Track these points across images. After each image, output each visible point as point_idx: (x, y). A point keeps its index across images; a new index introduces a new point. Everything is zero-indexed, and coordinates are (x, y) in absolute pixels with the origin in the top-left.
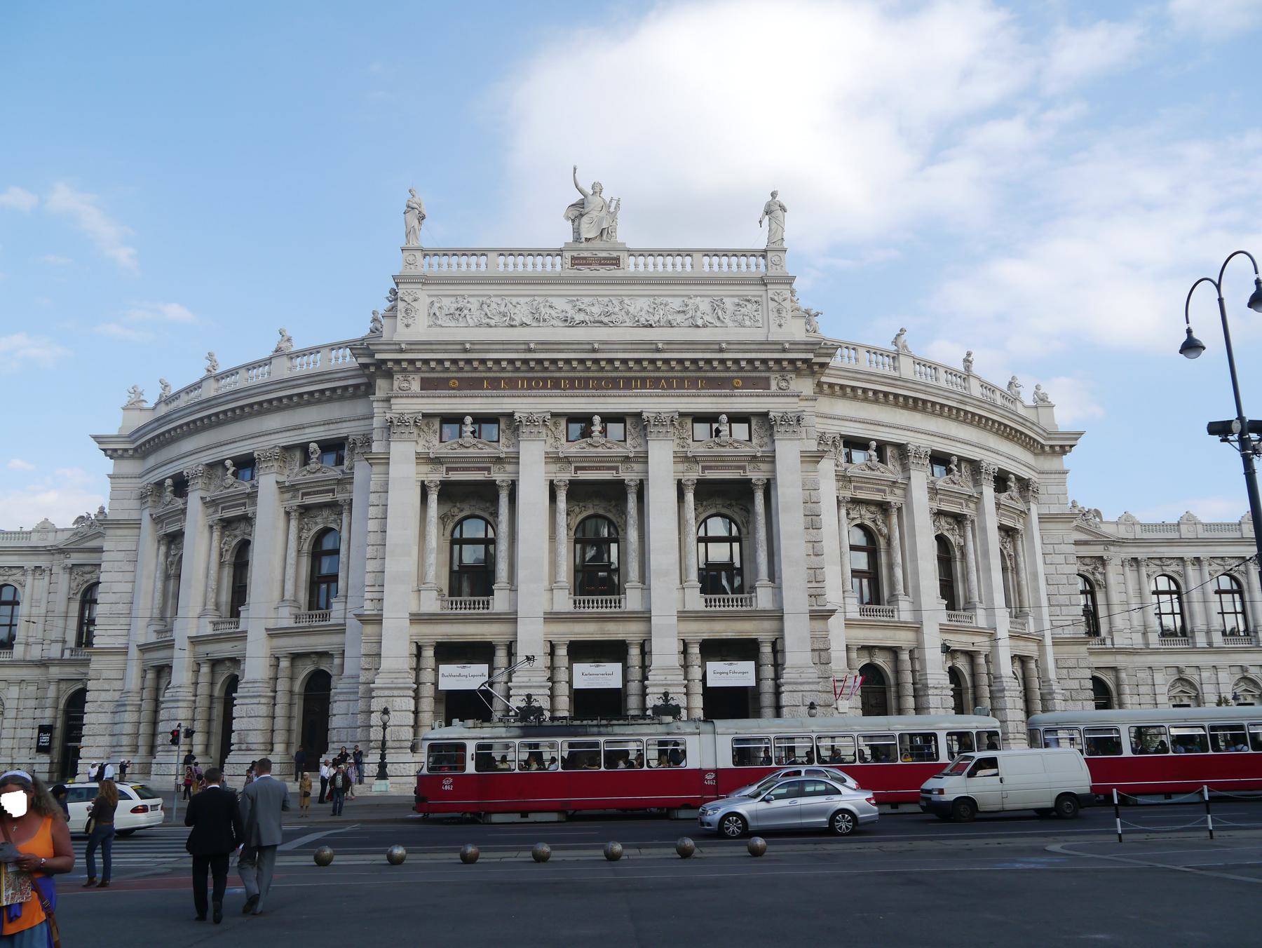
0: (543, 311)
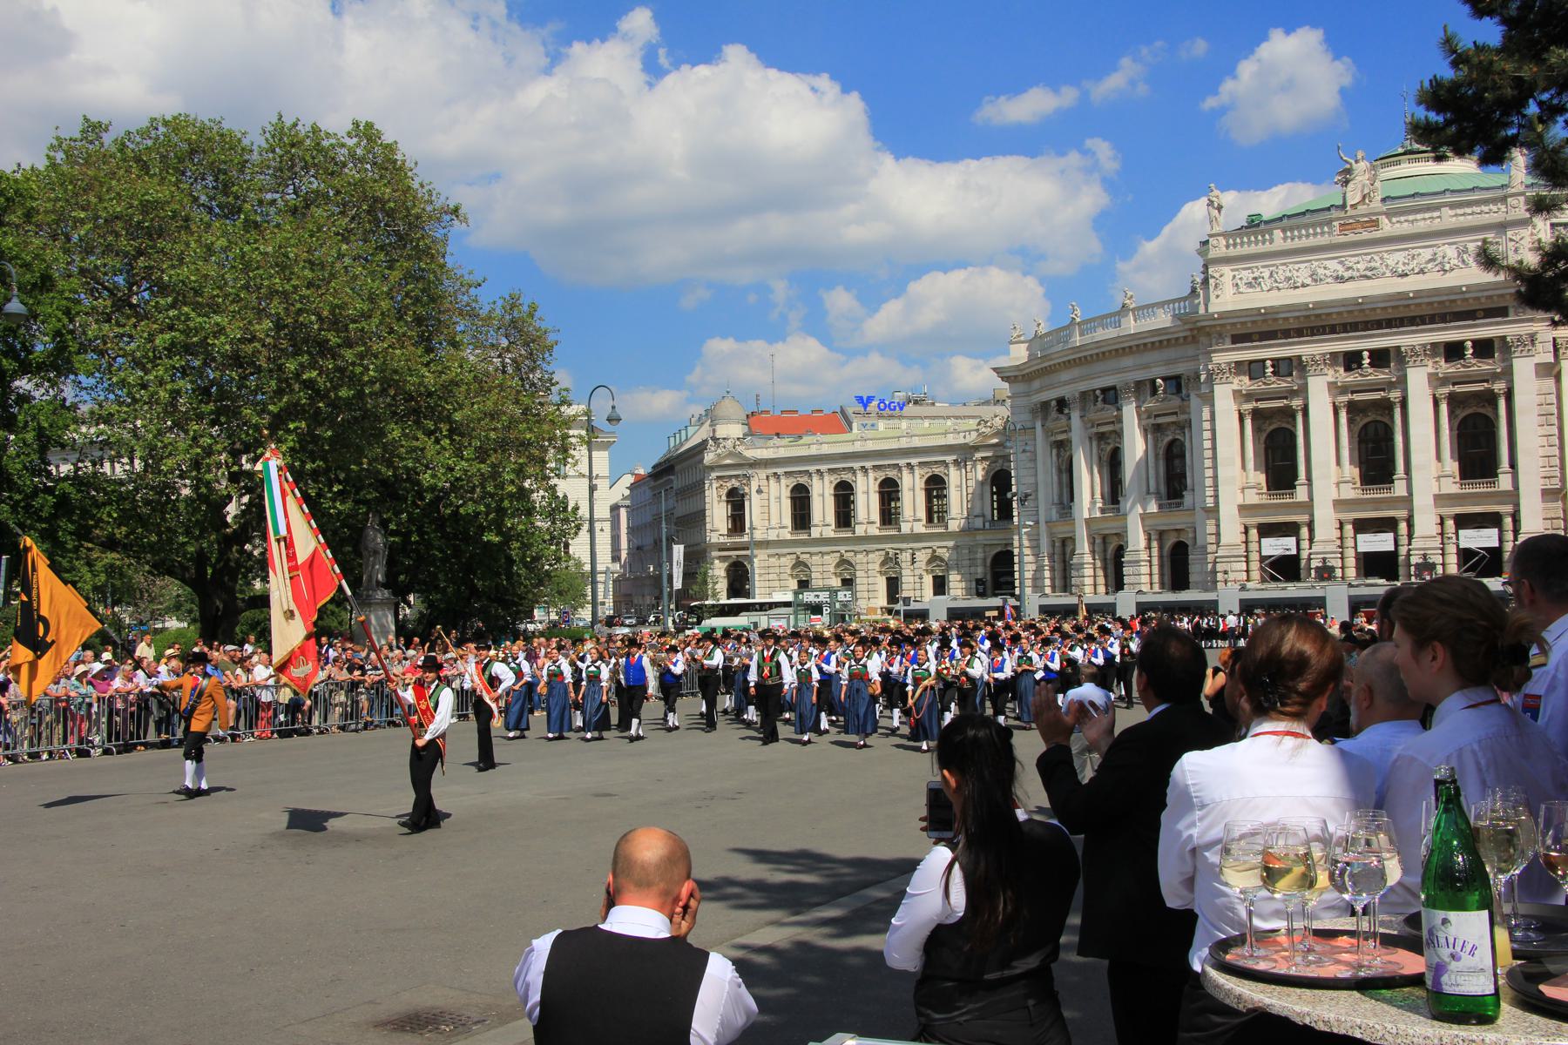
0: (1321, 271)
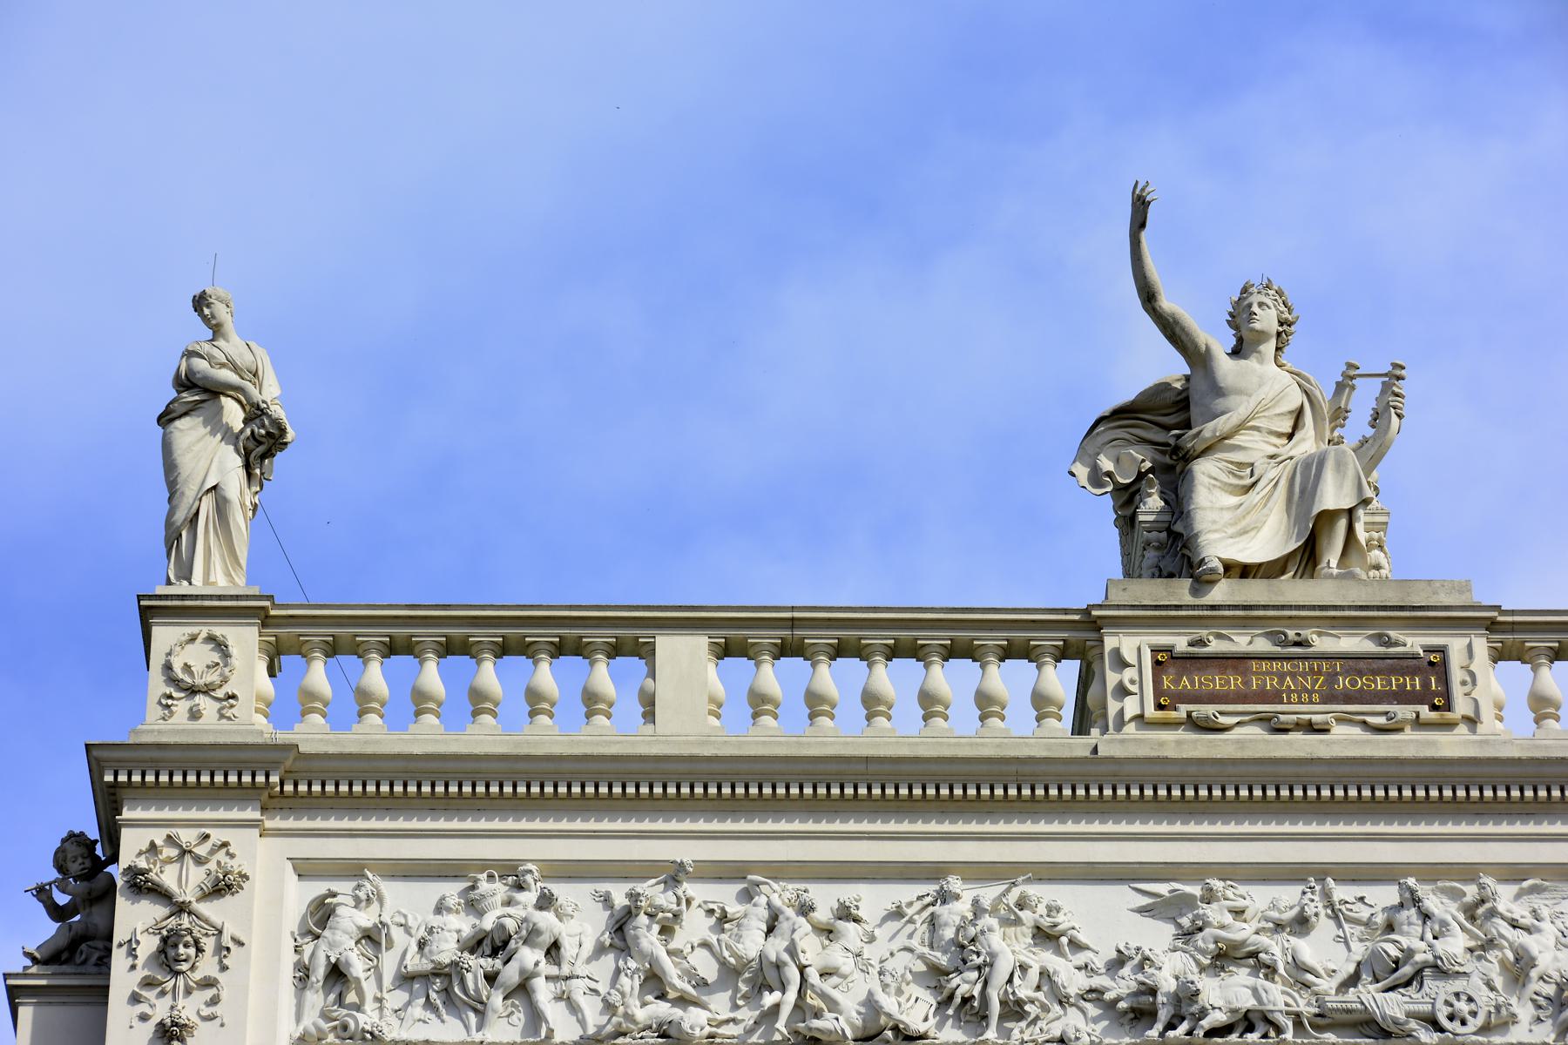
0: (1008, 948)
